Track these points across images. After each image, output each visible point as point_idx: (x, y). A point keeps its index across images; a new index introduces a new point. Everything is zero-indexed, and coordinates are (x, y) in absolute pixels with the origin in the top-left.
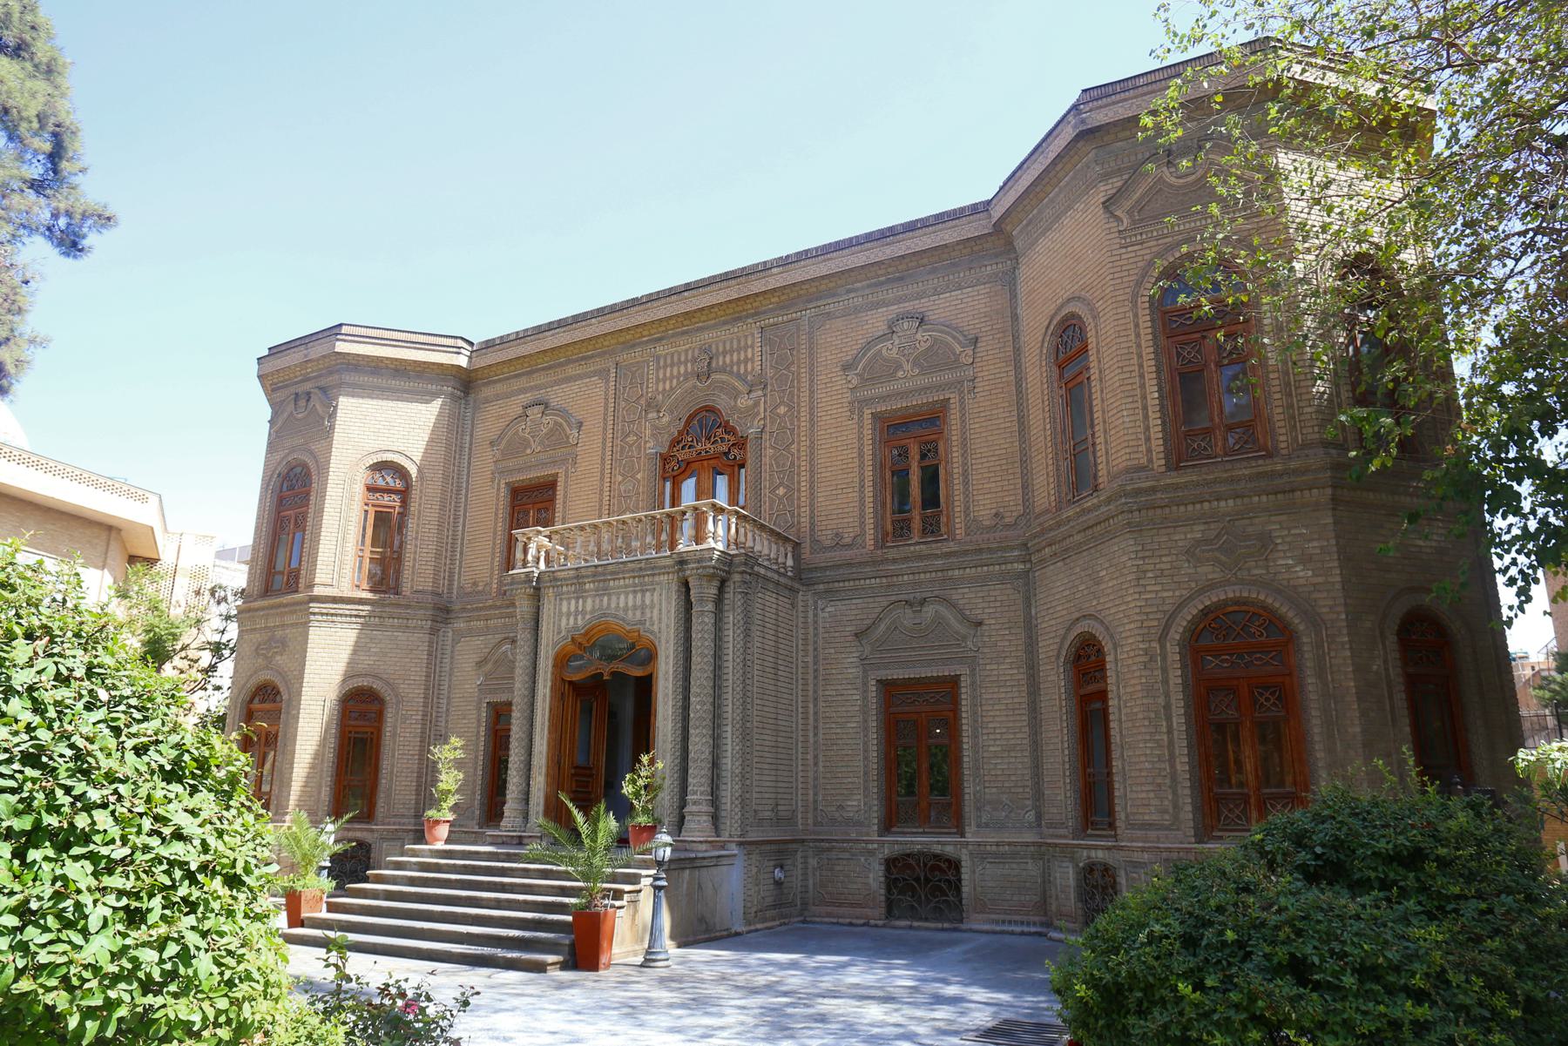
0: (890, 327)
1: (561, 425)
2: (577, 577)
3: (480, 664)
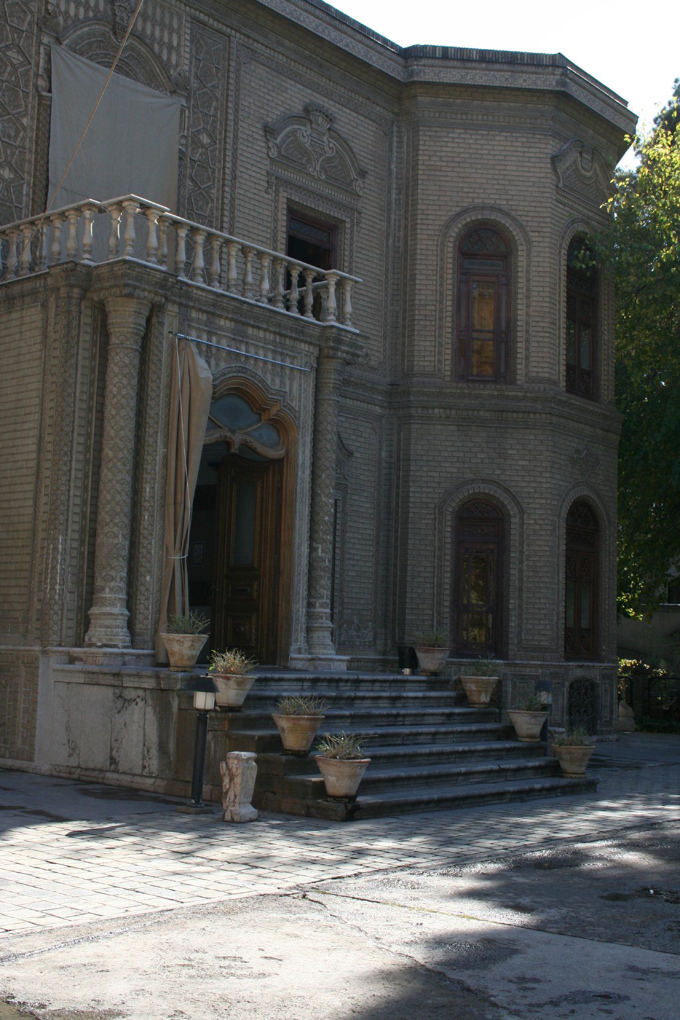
0: (306, 110)
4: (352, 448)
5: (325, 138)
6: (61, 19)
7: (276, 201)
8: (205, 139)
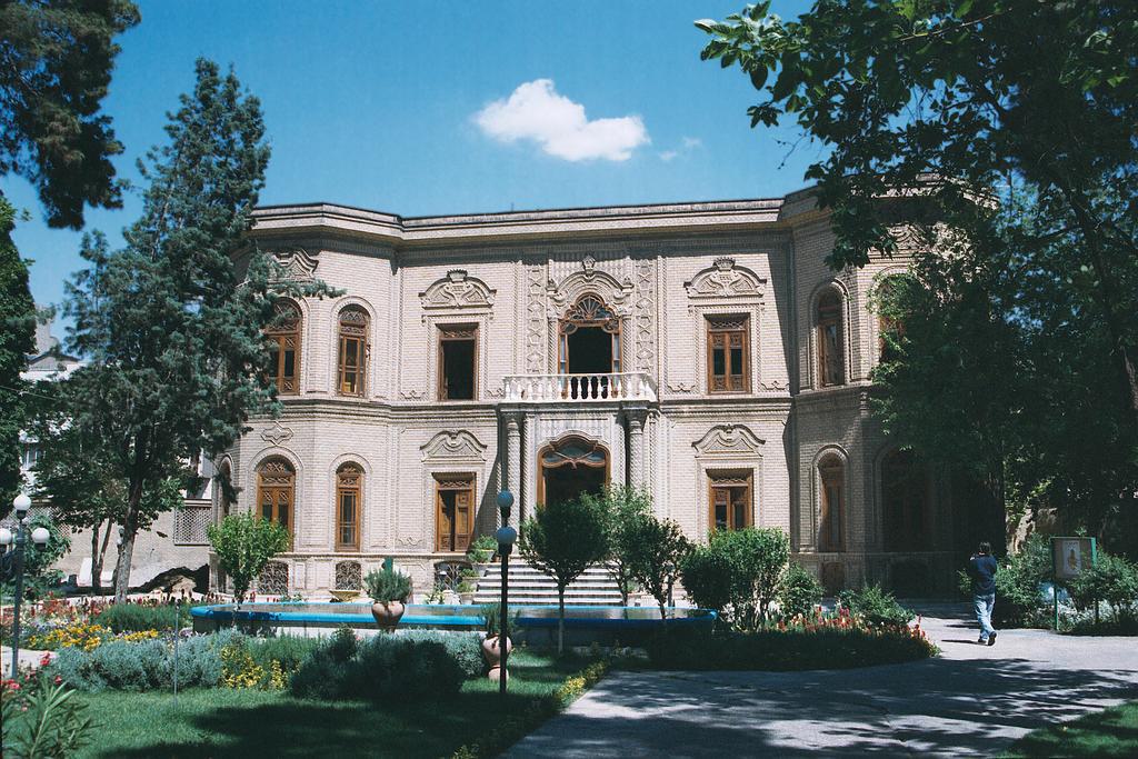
0: (715, 264)
6: (556, 282)
8: (645, 303)
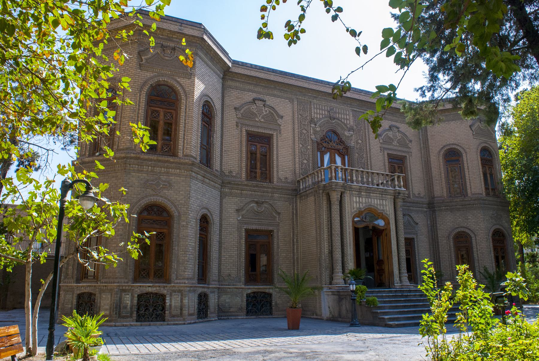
0: (390, 127)
1: (272, 113)
2: (360, 189)
3: (238, 211)
4: (417, 222)
5: (397, 134)
6: (316, 119)
7: (384, 154)
8: (360, 142)
